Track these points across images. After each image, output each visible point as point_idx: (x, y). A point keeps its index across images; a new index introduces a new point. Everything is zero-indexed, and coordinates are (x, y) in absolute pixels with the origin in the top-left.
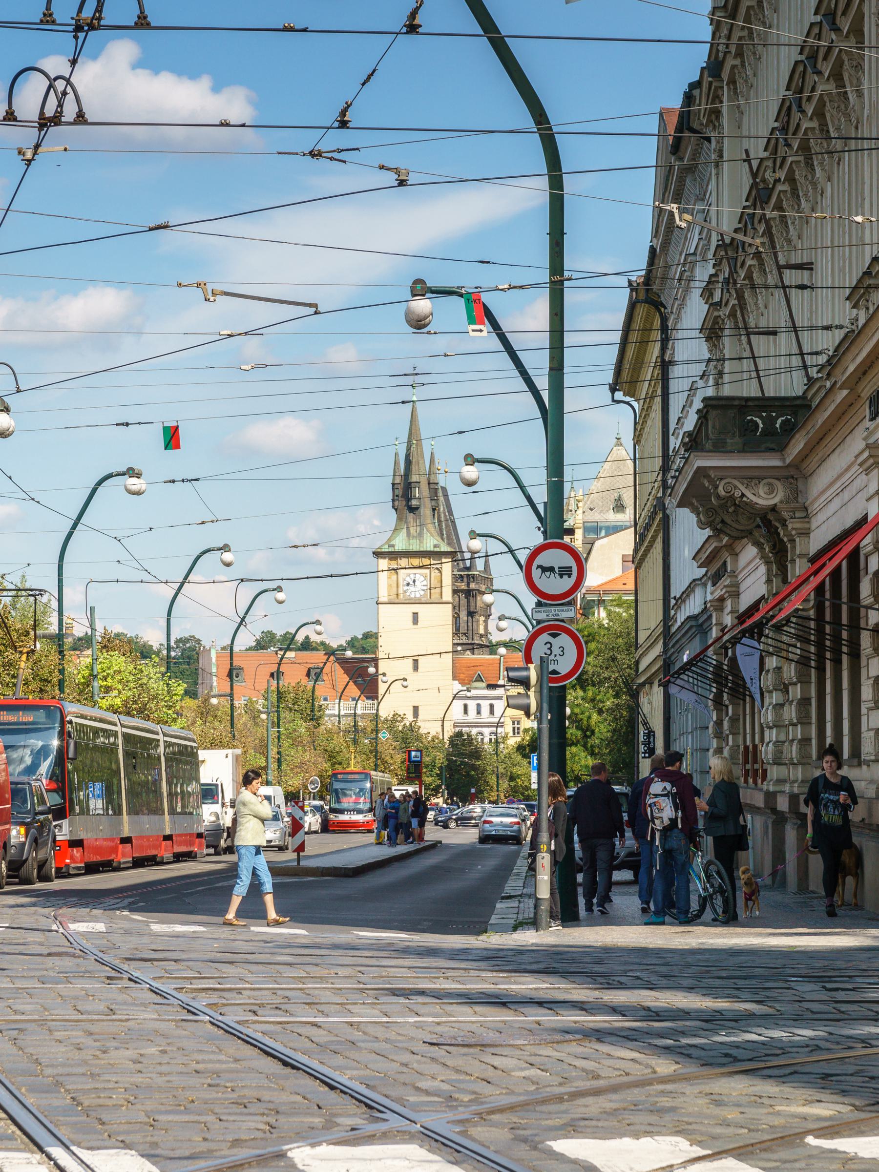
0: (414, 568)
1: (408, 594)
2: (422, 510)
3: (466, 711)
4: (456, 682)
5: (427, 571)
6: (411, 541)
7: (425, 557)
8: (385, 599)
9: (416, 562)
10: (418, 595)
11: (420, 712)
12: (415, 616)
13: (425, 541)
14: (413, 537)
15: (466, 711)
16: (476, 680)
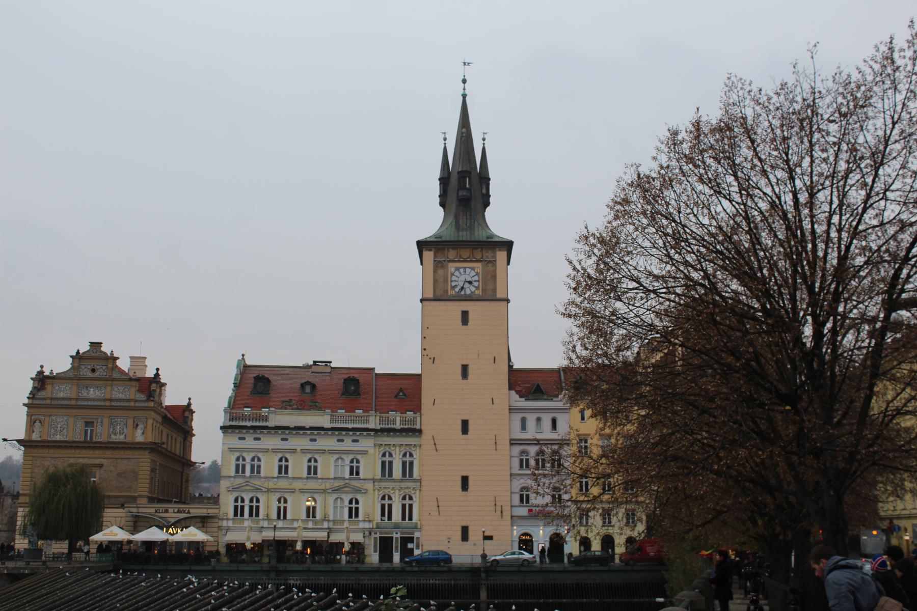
0: (465, 261)
1: (457, 289)
2: (473, 204)
3: (523, 428)
4: (513, 392)
5: (479, 265)
6: (461, 234)
7: (476, 249)
8: (431, 296)
9: (466, 253)
10: (468, 292)
11: (471, 426)
12: (465, 315)
13: (476, 234)
14: (463, 230)
15: (523, 428)
16: (534, 392)
